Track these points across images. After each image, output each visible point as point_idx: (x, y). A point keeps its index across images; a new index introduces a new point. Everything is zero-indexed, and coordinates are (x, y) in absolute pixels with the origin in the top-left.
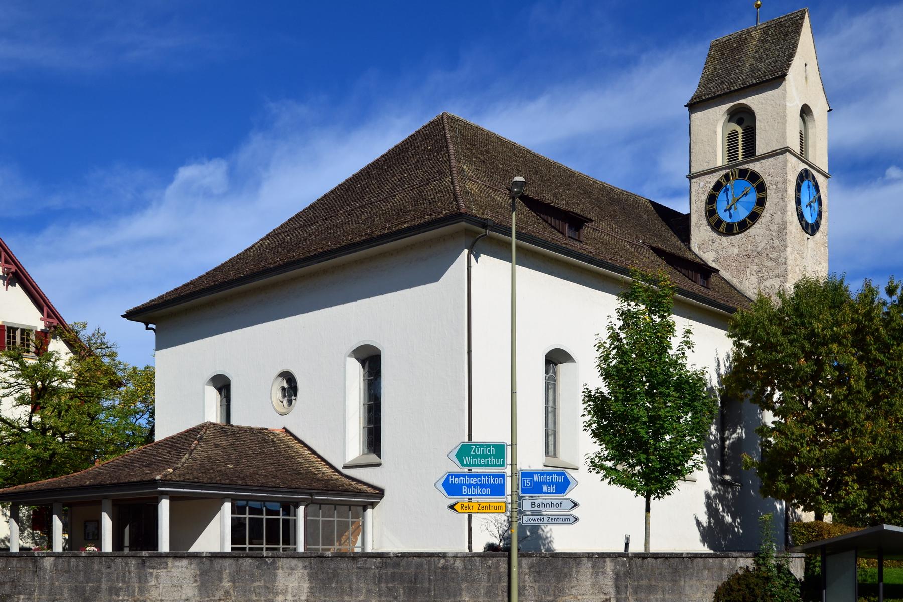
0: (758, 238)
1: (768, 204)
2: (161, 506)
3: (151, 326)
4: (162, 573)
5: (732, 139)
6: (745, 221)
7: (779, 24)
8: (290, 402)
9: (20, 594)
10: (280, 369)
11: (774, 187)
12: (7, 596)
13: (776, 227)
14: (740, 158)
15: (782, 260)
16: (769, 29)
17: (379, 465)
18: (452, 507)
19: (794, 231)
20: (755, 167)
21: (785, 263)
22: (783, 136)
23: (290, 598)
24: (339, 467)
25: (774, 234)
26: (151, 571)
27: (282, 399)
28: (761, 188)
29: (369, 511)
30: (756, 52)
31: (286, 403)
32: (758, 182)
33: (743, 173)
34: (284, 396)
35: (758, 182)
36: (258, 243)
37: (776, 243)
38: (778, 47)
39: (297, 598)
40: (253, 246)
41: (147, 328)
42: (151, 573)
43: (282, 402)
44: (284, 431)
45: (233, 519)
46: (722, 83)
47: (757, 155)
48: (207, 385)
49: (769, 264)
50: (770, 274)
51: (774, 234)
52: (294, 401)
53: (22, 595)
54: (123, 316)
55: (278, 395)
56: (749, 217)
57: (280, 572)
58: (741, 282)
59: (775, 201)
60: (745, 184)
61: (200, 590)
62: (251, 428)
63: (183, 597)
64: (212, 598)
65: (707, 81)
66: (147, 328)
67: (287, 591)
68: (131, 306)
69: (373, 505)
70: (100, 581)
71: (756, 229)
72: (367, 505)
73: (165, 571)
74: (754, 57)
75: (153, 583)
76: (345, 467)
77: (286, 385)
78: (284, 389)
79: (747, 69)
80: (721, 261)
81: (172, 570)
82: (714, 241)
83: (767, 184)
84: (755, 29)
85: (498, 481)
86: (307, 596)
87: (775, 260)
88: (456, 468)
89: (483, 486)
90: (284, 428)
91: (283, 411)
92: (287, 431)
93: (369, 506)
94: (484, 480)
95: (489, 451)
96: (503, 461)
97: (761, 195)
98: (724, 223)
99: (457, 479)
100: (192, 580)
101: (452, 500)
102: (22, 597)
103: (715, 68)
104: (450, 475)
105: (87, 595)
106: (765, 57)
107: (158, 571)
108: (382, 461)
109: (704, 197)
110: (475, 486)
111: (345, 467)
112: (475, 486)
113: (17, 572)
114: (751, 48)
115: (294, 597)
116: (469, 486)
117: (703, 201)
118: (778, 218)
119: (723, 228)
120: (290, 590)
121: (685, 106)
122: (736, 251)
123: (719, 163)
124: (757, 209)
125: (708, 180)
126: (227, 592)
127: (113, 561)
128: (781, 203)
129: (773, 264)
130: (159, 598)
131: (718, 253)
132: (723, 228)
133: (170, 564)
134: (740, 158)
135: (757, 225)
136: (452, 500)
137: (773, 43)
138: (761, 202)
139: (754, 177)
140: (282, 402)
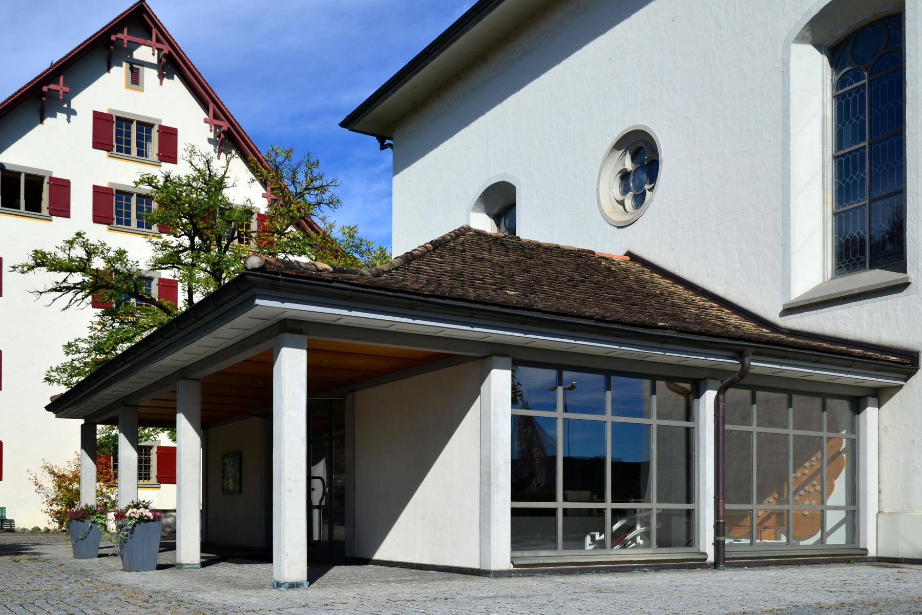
2: (280, 368)
8: (640, 200)
10: (618, 132)
17: (901, 287)
24: (772, 313)
27: (620, 198)
29: (871, 413)
31: (629, 202)
34: (625, 190)
41: (383, 147)
43: (622, 203)
44: (628, 258)
48: (474, 210)
52: (648, 193)
55: (611, 188)
62: (558, 247)
69: (880, 395)
72: (865, 397)
76: (789, 310)
77: (629, 165)
78: (625, 176)
90: (629, 254)
91: (622, 218)
93: (871, 400)
108: (912, 273)
111: (789, 310)
140: (622, 203)
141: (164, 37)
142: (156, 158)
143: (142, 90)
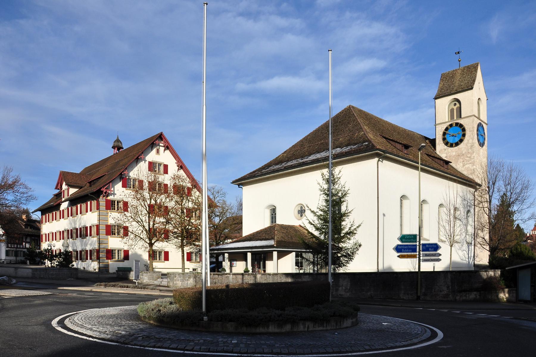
0: (463, 149)
1: (466, 136)
3: (240, 186)
5: (452, 111)
6: (458, 142)
7: (468, 67)
8: (301, 216)
11: (469, 130)
13: (470, 145)
14: (455, 118)
15: (472, 157)
18: (399, 256)
19: (476, 146)
20: (461, 121)
21: (474, 159)
22: (472, 110)
23: (344, 288)
25: (469, 147)
28: (464, 130)
30: (460, 78)
32: (462, 128)
33: (457, 124)
34: (299, 213)
35: (462, 128)
36: (281, 155)
37: (470, 151)
38: (469, 77)
39: (346, 288)
40: (279, 156)
41: (239, 187)
45: (296, 259)
46: (447, 90)
47: (462, 117)
49: (468, 158)
50: (468, 162)
51: (469, 147)
54: (231, 183)
56: (459, 141)
57: (341, 279)
58: (456, 165)
59: (469, 135)
60: (458, 128)
62: (289, 225)
65: (441, 90)
66: (239, 187)
67: (343, 286)
68: (234, 179)
71: (462, 145)
74: (459, 81)
79: (457, 84)
80: (448, 157)
81: (303, 279)
82: (445, 150)
83: (466, 128)
84: (459, 69)
85: (414, 247)
86: (350, 287)
87: (470, 157)
88: (400, 243)
89: (409, 249)
90: (300, 225)
91: (299, 218)
92: (301, 226)
94: (410, 247)
95: (411, 237)
96: (416, 240)
97: (464, 133)
98: (449, 143)
99: (400, 247)
101: (399, 254)
103: (444, 84)
104: (398, 245)
109: (441, 133)
110: (407, 249)
112: (407, 249)
113: (247, 279)
114: (458, 76)
115: (345, 287)
116: (404, 249)
117: (440, 135)
118: (471, 141)
119: (449, 144)
120: (344, 285)
121: (433, 99)
122: (454, 154)
123: (447, 121)
124: (462, 138)
125: (442, 127)
127: (282, 276)
128: (472, 136)
129: (469, 159)
131: (447, 154)
132: (449, 144)
133: (302, 277)
134: (455, 118)
135: (462, 144)
136: (399, 254)
137: (467, 75)
138: (464, 135)
139: (461, 126)
141: (166, 141)
142: (163, 173)
143: (160, 155)
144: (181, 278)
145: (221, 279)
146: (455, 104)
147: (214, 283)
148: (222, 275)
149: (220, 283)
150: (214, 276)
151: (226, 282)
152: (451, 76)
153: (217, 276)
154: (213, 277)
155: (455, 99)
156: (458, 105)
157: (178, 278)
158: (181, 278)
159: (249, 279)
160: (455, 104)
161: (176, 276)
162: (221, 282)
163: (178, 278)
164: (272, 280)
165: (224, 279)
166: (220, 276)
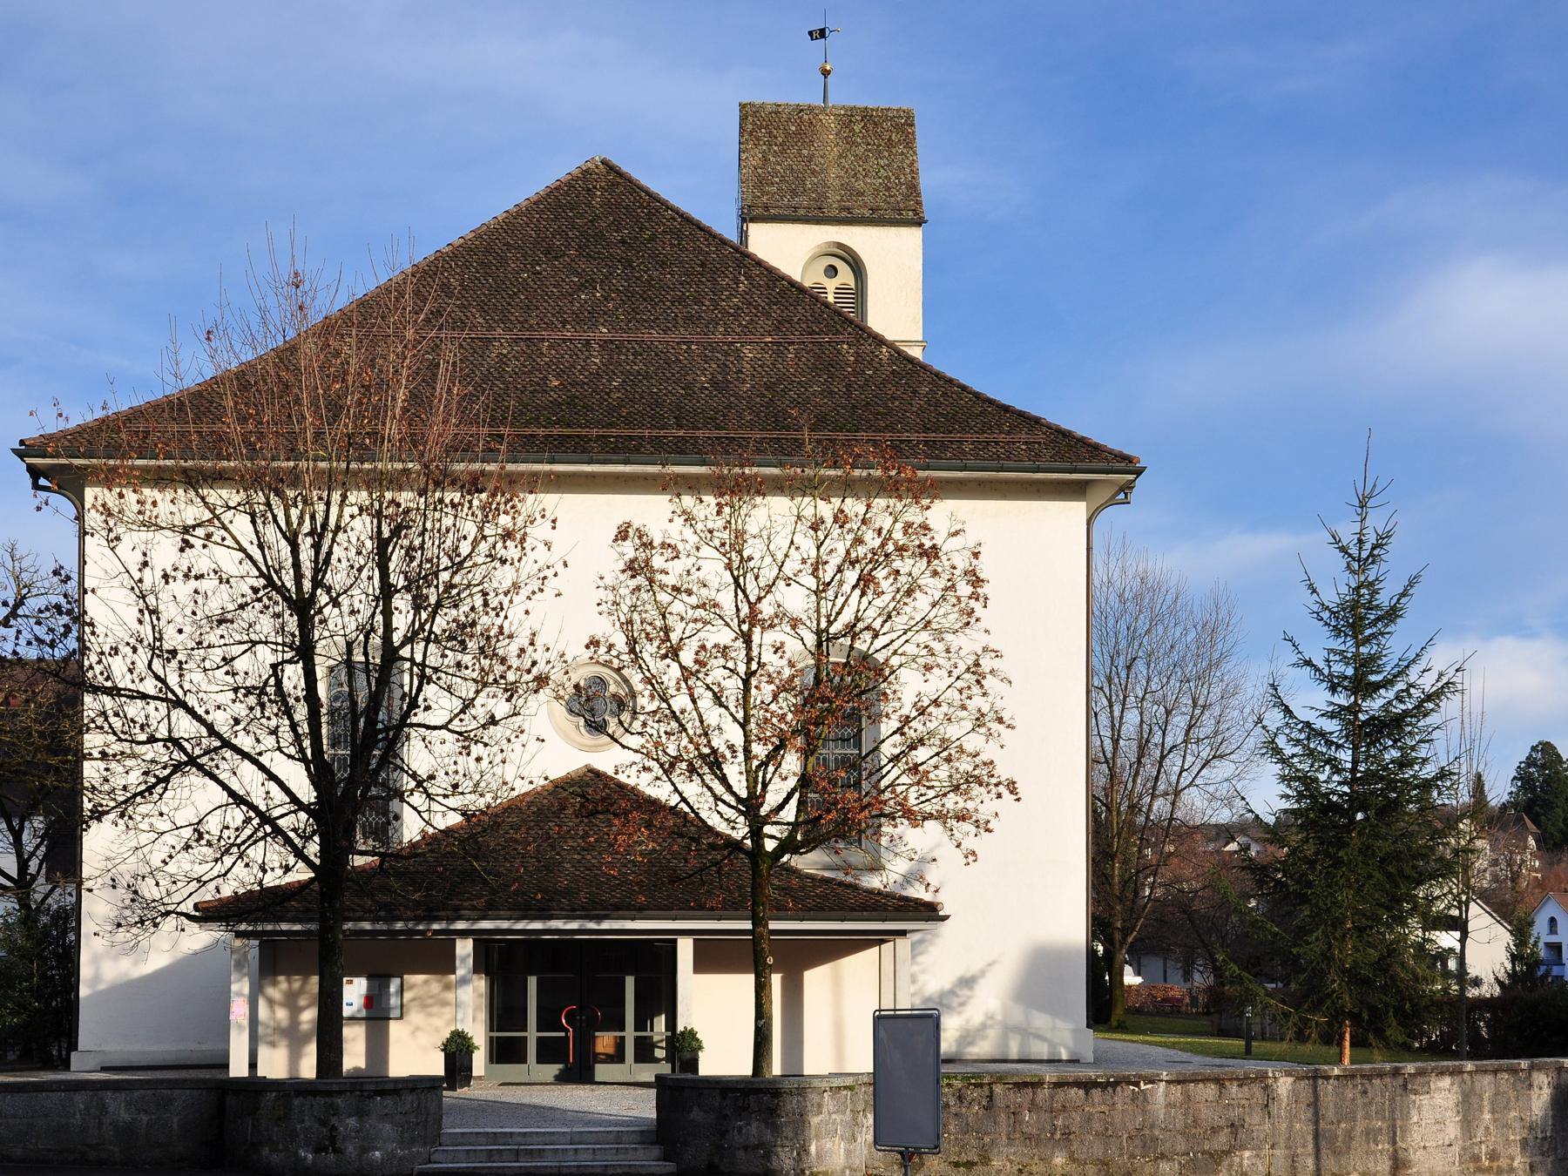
4: (1424, 1100)
9: (1243, 1147)
12: (1223, 1152)
16: (851, 121)
26: (1414, 1097)
30: (840, 156)
42: (1414, 1102)
53: (1248, 1149)
61: (1462, 1128)
63: (1447, 1143)
64: (1474, 1140)
70: (1354, 1119)
73: (1428, 1096)
75: (1415, 1119)
100: (1454, 1110)
102: (1247, 1154)
105: (1338, 1144)
106: (864, 173)
107: (1421, 1098)
126: (1487, 1128)
130: (1422, 1144)
144: (844, 1113)
145: (1102, 1108)
146: (832, 271)
147: (1058, 1136)
148: (1110, 1089)
149: (1097, 1134)
150: (1061, 1094)
151: (1131, 1128)
152: (794, 128)
153: (1081, 1092)
154: (1052, 1097)
155: (840, 245)
156: (846, 276)
157: (830, 1114)
158: (844, 1113)
159: (1244, 1102)
160: (832, 271)
161: (820, 1105)
162: (1101, 1129)
163: (830, 1114)
164: (1336, 1104)
165: (1119, 1106)
166: (1096, 1093)
